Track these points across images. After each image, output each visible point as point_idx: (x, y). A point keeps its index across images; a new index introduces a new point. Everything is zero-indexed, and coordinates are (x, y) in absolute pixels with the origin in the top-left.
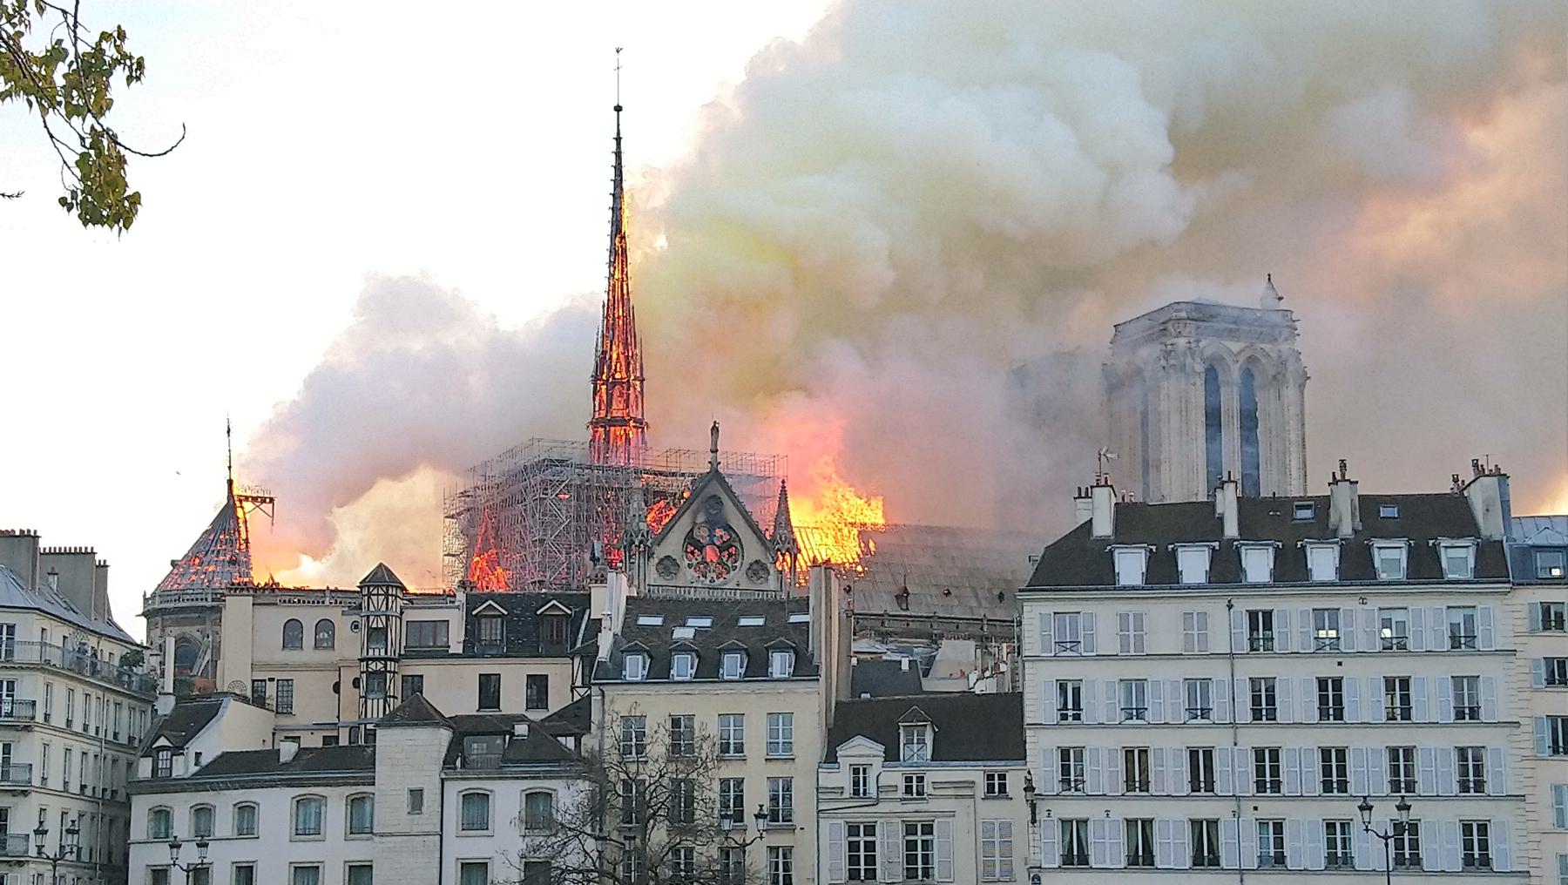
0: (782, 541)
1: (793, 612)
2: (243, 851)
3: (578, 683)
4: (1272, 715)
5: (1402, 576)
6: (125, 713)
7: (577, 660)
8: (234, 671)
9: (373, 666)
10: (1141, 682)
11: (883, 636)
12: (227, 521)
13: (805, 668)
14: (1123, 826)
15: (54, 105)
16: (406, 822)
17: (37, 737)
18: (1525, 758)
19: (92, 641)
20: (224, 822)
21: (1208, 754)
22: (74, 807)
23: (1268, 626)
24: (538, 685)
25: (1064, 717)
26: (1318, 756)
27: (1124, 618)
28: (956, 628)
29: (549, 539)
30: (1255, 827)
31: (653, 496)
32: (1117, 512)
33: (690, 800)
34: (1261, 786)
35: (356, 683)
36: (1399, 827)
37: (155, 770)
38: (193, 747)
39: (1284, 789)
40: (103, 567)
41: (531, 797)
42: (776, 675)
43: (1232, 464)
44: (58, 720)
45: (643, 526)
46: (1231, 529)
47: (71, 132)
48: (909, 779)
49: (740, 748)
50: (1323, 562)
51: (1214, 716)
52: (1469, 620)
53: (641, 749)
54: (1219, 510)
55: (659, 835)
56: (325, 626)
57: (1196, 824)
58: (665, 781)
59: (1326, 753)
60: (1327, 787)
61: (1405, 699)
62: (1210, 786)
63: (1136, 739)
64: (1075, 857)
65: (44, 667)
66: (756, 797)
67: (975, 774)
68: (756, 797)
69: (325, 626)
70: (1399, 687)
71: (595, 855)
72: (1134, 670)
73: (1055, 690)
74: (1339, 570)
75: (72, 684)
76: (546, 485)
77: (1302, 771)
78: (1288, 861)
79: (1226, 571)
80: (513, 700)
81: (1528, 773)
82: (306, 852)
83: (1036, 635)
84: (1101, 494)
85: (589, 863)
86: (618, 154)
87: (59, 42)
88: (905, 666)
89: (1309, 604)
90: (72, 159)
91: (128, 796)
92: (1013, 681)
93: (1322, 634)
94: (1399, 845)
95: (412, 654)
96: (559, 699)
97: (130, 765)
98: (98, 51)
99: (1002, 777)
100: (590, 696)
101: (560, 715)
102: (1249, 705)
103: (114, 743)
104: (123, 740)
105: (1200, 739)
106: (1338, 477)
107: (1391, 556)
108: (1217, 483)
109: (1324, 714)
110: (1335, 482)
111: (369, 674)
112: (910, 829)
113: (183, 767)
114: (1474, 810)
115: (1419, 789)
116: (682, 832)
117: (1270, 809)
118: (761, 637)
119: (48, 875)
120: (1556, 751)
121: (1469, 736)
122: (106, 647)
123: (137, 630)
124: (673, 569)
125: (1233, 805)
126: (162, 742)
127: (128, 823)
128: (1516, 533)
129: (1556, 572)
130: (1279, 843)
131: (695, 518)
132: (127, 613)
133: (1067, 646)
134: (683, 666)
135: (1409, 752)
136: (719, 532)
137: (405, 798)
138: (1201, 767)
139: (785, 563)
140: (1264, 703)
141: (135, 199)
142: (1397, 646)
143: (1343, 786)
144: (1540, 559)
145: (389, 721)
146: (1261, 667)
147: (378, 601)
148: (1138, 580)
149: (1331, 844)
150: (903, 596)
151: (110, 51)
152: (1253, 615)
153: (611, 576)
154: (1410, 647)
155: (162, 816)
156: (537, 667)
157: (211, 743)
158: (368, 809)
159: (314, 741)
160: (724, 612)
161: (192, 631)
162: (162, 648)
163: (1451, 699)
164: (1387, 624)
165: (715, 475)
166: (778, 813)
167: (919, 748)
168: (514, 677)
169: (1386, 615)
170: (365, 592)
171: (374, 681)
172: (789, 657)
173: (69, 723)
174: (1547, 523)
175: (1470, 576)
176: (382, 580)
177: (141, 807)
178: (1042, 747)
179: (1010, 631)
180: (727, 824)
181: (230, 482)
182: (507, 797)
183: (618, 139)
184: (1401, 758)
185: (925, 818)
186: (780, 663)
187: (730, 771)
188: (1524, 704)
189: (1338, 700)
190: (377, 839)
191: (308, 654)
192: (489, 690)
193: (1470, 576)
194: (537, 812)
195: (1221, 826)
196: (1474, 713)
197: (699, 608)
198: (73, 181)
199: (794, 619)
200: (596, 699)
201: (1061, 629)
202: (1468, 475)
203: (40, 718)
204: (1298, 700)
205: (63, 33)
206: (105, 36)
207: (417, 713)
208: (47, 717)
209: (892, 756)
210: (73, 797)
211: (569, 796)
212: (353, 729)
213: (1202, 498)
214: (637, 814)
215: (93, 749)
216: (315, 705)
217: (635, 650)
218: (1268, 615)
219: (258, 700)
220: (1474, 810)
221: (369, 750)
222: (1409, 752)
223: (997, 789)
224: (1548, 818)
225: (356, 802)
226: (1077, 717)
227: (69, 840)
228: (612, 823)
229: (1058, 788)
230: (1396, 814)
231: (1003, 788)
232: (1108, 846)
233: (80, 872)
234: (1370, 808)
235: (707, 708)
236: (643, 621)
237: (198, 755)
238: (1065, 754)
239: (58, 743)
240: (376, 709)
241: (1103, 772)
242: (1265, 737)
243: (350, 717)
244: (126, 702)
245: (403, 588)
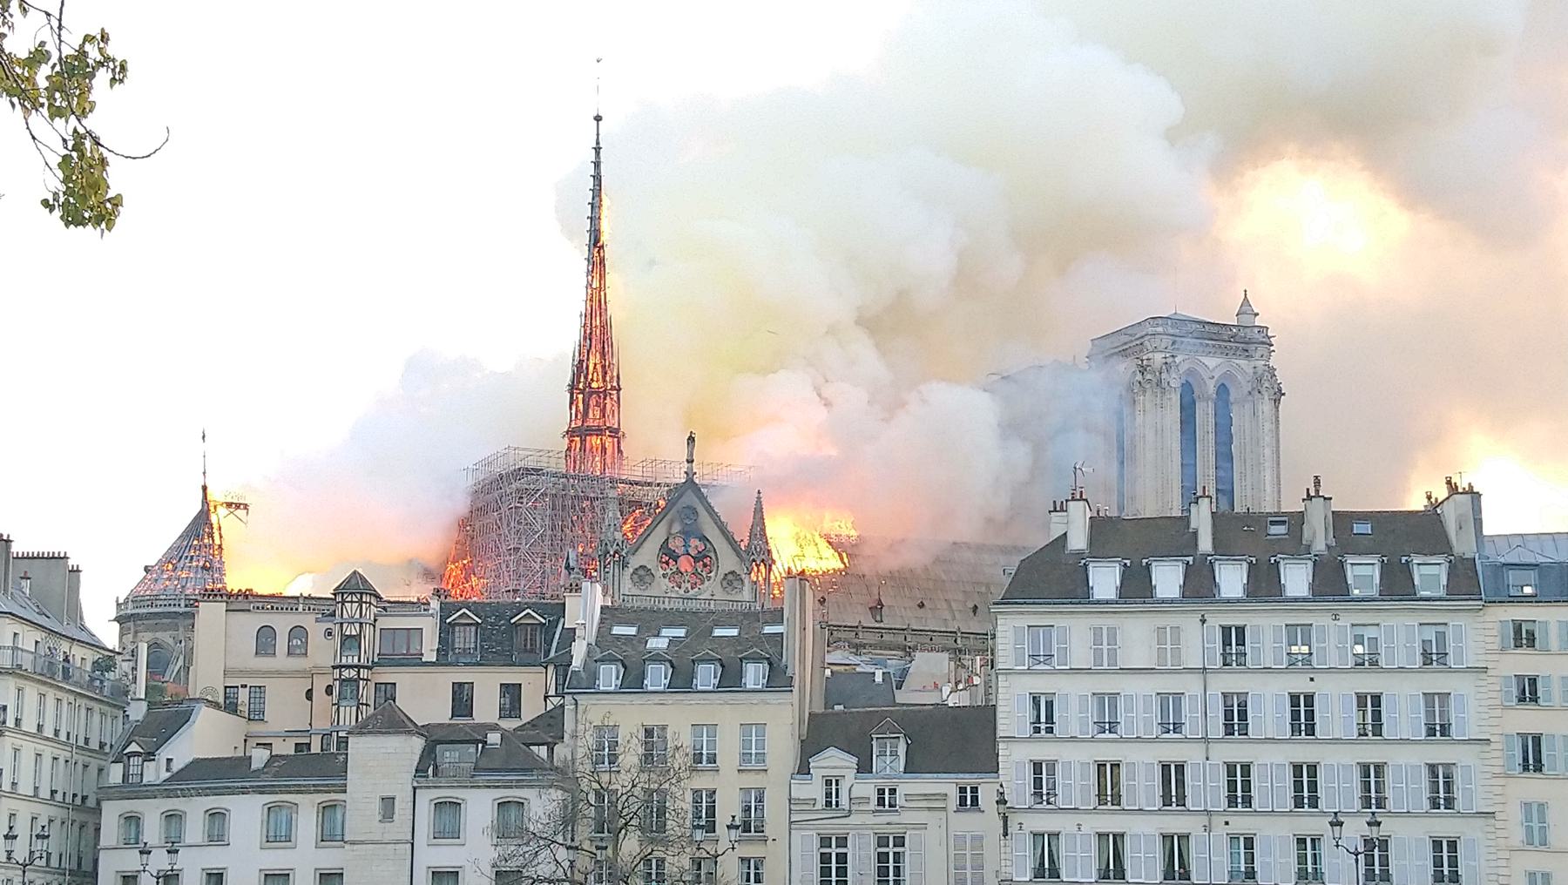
0: (757, 552)
1: (766, 623)
2: (214, 858)
3: (552, 692)
4: (1244, 731)
5: (1375, 592)
6: (96, 718)
7: (551, 669)
8: (207, 676)
9: (346, 674)
10: (1114, 696)
11: (857, 648)
12: (202, 524)
13: (778, 679)
14: (1094, 841)
15: (36, 106)
16: (376, 829)
18: (1496, 776)
19: (65, 646)
20: (195, 829)
21: (1180, 768)
22: (44, 813)
23: (1241, 642)
24: (512, 694)
25: (1037, 730)
26: (1289, 772)
27: (1097, 632)
28: (930, 640)
29: (524, 548)
30: (1226, 840)
31: (629, 505)
32: (1091, 527)
33: (662, 812)
34: (1232, 801)
35: (329, 690)
36: (1368, 842)
37: (125, 777)
38: (163, 754)
39: (1255, 804)
40: (76, 571)
42: (750, 686)
43: (1206, 477)
44: (29, 725)
45: (618, 536)
46: (1205, 544)
47: (54, 134)
48: (881, 792)
49: (712, 759)
50: (1296, 578)
51: (1186, 730)
52: (1441, 637)
53: (613, 759)
54: (1193, 525)
55: (631, 845)
56: (298, 632)
57: (1167, 838)
58: (637, 791)
59: (1297, 769)
60: (1299, 803)
61: (1377, 715)
62: (1181, 801)
63: (1108, 753)
66: (728, 808)
67: (947, 786)
68: (728, 808)
69: (298, 632)
70: (1372, 704)
71: (566, 864)
72: (1107, 684)
73: (1029, 703)
74: (1312, 587)
75: (44, 689)
76: (521, 494)
77: (1272, 787)
78: (1258, 876)
79: (1200, 586)
80: (486, 708)
81: (1499, 790)
82: (276, 860)
83: (1010, 647)
84: (1076, 508)
85: (560, 873)
86: (597, 164)
87: (42, 44)
88: (879, 678)
89: (1281, 620)
90: (55, 160)
91: (98, 803)
92: (987, 694)
93: (1295, 649)
94: (1370, 862)
95: (385, 661)
96: (532, 708)
97: (100, 770)
98: (82, 53)
99: (974, 790)
100: (562, 706)
101: (532, 724)
102: (1221, 720)
103: (85, 747)
104: (94, 745)
105: (1173, 753)
106: (1312, 493)
107: (1363, 572)
108: (1192, 497)
109: (1295, 729)
110: (1309, 497)
111: (343, 681)
112: (882, 841)
113: (154, 773)
114: (1445, 827)
115: (1390, 805)
116: (652, 841)
117: (1242, 824)
118: (736, 650)
119: (17, 881)
120: (1526, 768)
121: (1440, 753)
122: (78, 653)
123: (109, 636)
124: (647, 579)
125: (1204, 820)
126: (133, 747)
127: (98, 830)
128: (1488, 550)
129: (1528, 590)
130: (1250, 859)
131: (670, 527)
132: (100, 619)
133: (1041, 659)
134: (658, 676)
135: (1379, 768)
136: (694, 542)
137: (376, 806)
138: (1173, 779)
139: (759, 574)
140: (1236, 718)
141: (117, 202)
142: (1367, 663)
143: (1314, 803)
144: (1512, 577)
145: (362, 729)
146: (1234, 682)
147: (351, 609)
148: (1112, 594)
149: (1302, 859)
150: (877, 609)
151: (93, 53)
152: (1226, 630)
153: (586, 585)
154: (1383, 663)
155: (133, 820)
156: (511, 676)
157: (183, 749)
158: (339, 816)
159: (286, 748)
160: (699, 622)
161: (165, 637)
162: (134, 653)
163: (1422, 715)
164: (1359, 640)
166: (749, 825)
167: (891, 759)
168: (487, 685)
169: (1359, 631)
170: (339, 599)
172: (763, 668)
173: (40, 727)
174: (1518, 541)
175: (1442, 593)
176: (355, 587)
177: (112, 813)
178: (1014, 759)
179: (985, 643)
180: (699, 835)
181: (205, 488)
182: (479, 806)
183: (597, 150)
184: (1372, 775)
185: (898, 830)
186: (754, 674)
187: (702, 782)
188: (1494, 722)
189: (1310, 715)
190: (347, 847)
191: (281, 661)
192: (462, 700)
193: (1442, 593)
195: (1192, 840)
196: (1445, 730)
197: (673, 618)
198: (54, 183)
199: (768, 630)
200: (569, 708)
201: (1035, 643)
202: (1441, 493)
203: (10, 723)
204: (1269, 715)
205: (46, 35)
206: (88, 39)
207: (390, 721)
208: (18, 721)
209: (864, 767)
210: (43, 802)
211: (541, 805)
212: (326, 736)
213: (1177, 513)
214: (609, 826)
215: (63, 755)
216: (287, 712)
217: (610, 660)
218: (1241, 631)
219: (231, 707)
220: (1445, 827)
221: (341, 758)
222: (1379, 768)
223: (968, 800)
224: (1518, 835)
225: (327, 809)
226: (1050, 730)
227: (39, 845)
228: (584, 832)
229: (1029, 800)
230: (1366, 831)
231: (975, 800)
233: (49, 877)
234: (1341, 824)
235: (679, 719)
236: (617, 630)
237: (169, 760)
238: (1037, 766)
239: (29, 748)
240: (348, 716)
241: (1076, 785)
242: (1237, 752)
243: (321, 724)
244: (96, 706)
245: (378, 597)
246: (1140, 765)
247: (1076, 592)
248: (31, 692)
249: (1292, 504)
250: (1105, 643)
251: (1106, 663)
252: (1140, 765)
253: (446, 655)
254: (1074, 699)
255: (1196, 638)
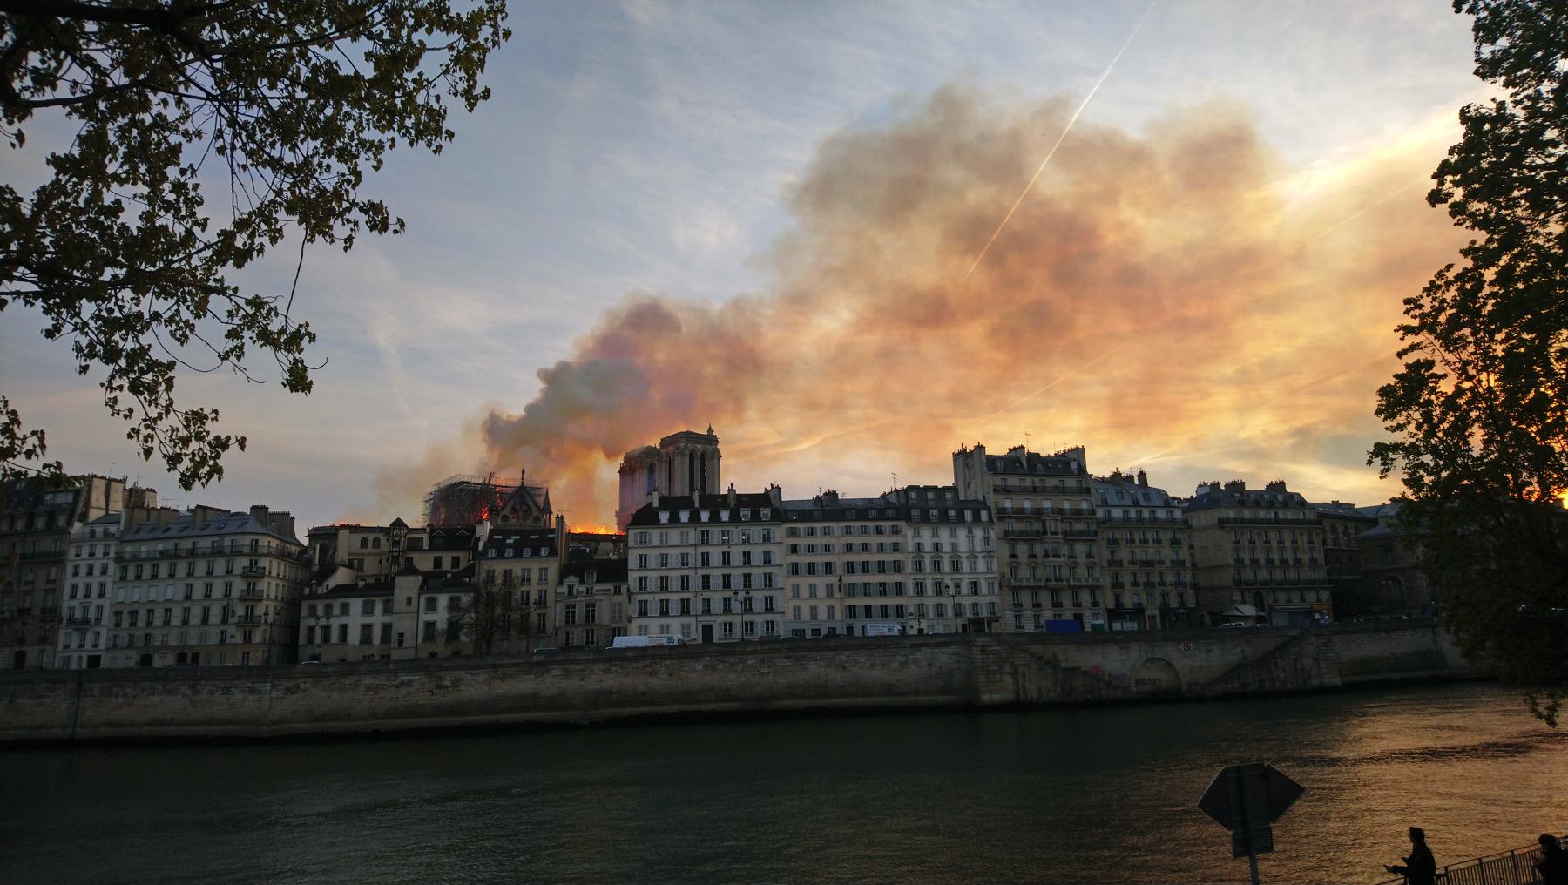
2: (344, 620)
8: (342, 554)
13: (553, 553)
17: (266, 580)
41: (452, 599)
44: (274, 574)
47: (285, 358)
56: (377, 540)
63: (664, 573)
64: (643, 613)
65: (269, 555)
69: (377, 540)
72: (664, 551)
79: (695, 518)
80: (446, 564)
82: (368, 620)
96: (463, 565)
105: (684, 573)
107: (746, 513)
108: (692, 489)
113: (321, 590)
123: (305, 542)
133: (643, 543)
134: (509, 553)
138: (685, 581)
145: (400, 573)
155: (313, 609)
157: (332, 582)
160: (524, 534)
165: (523, 486)
171: (395, 560)
176: (398, 523)
178: (633, 577)
186: (544, 551)
191: (370, 549)
194: (454, 605)
197: (516, 532)
204: (716, 559)
207: (410, 570)
209: (582, 582)
211: (466, 599)
213: (687, 493)
216: (371, 567)
219: (350, 565)
232: (654, 609)
235: (517, 568)
239: (274, 583)
240: (395, 569)
241: (653, 584)
246: (675, 576)
247: (655, 521)
248: (275, 563)
249: (724, 491)
250: (664, 537)
251: (664, 544)
252: (675, 576)
253: (432, 547)
254: (653, 555)
255: (693, 535)
